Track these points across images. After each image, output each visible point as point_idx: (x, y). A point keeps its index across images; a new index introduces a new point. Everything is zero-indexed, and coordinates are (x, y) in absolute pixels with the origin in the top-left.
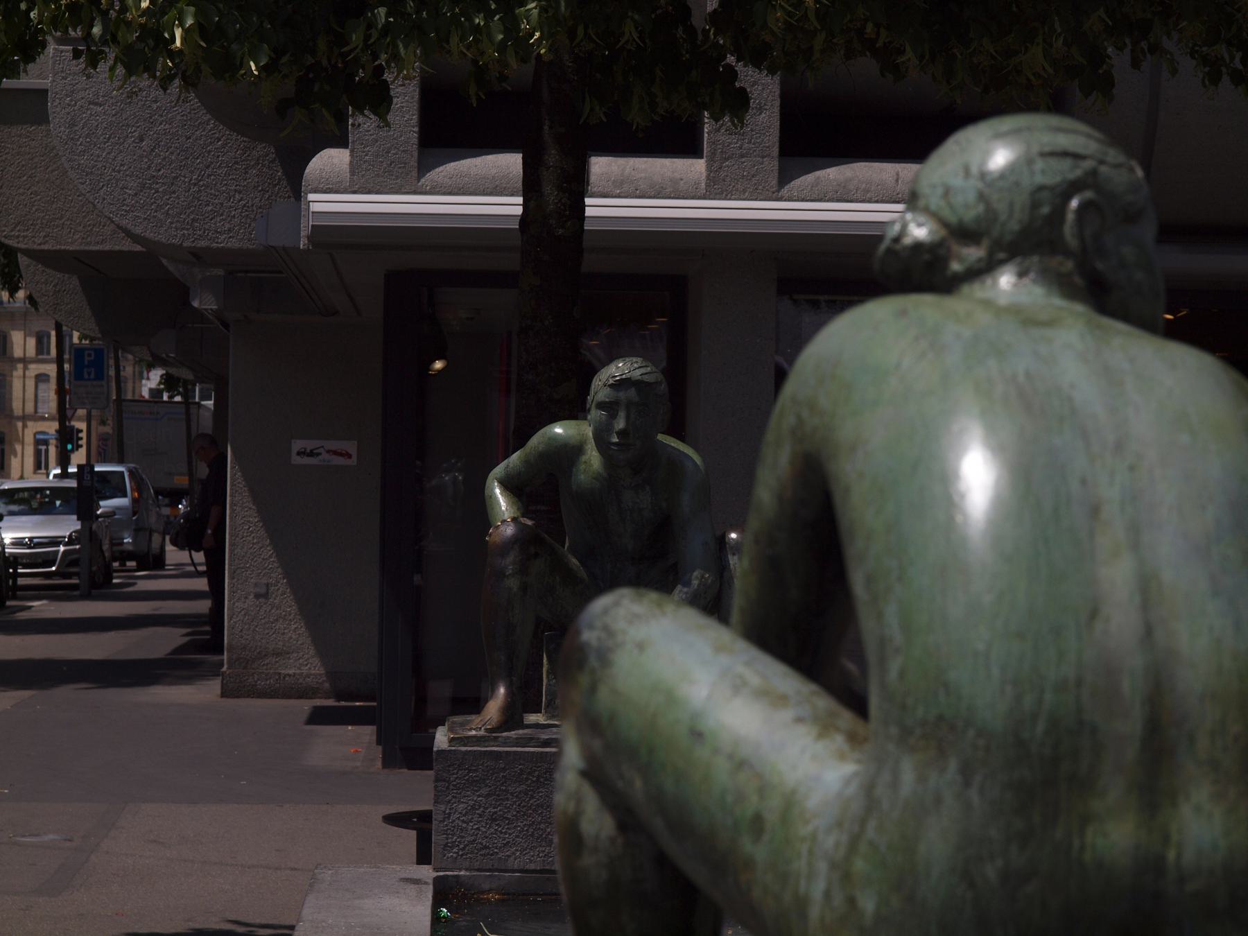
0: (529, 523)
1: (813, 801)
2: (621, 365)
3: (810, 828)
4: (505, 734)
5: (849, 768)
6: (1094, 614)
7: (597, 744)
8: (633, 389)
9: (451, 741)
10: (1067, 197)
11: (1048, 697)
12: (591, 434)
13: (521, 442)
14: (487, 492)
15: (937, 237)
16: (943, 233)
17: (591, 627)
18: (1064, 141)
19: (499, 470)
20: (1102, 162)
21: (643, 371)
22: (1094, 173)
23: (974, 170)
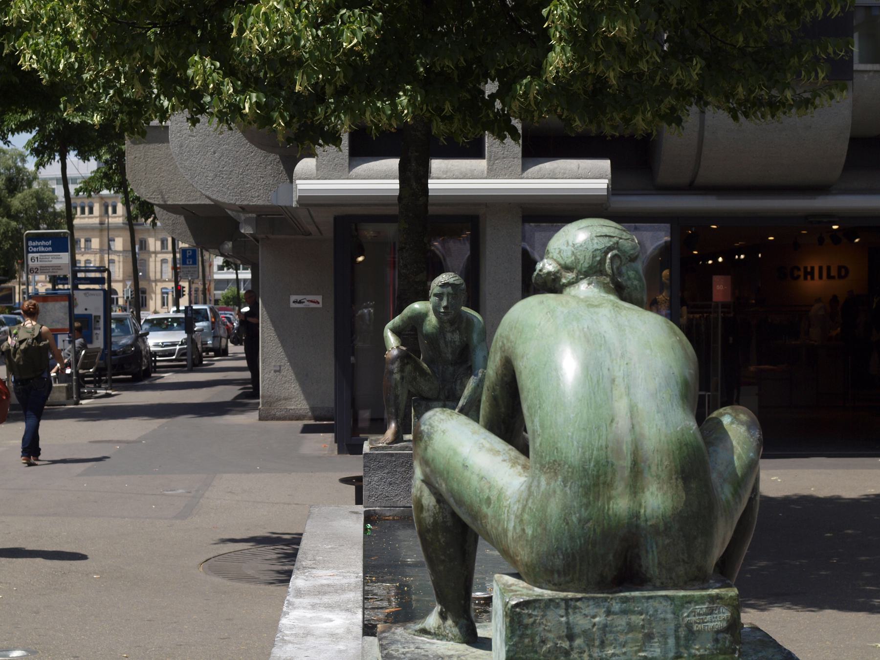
0: (404, 348)
1: (509, 493)
2: (444, 276)
3: (508, 502)
4: (395, 445)
5: (523, 479)
6: (612, 421)
7: (428, 470)
8: (450, 287)
9: (371, 448)
10: (606, 253)
11: (595, 452)
12: (431, 308)
13: (399, 311)
14: (385, 335)
15: (556, 270)
16: (559, 267)
17: (425, 424)
18: (606, 231)
19: (390, 325)
20: (621, 238)
21: (454, 279)
22: (617, 243)
23: (571, 243)
